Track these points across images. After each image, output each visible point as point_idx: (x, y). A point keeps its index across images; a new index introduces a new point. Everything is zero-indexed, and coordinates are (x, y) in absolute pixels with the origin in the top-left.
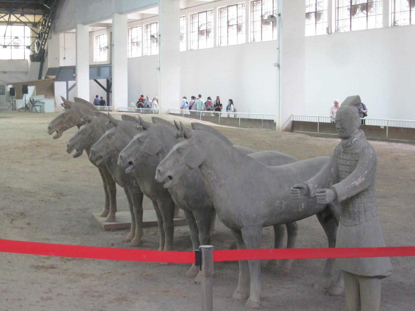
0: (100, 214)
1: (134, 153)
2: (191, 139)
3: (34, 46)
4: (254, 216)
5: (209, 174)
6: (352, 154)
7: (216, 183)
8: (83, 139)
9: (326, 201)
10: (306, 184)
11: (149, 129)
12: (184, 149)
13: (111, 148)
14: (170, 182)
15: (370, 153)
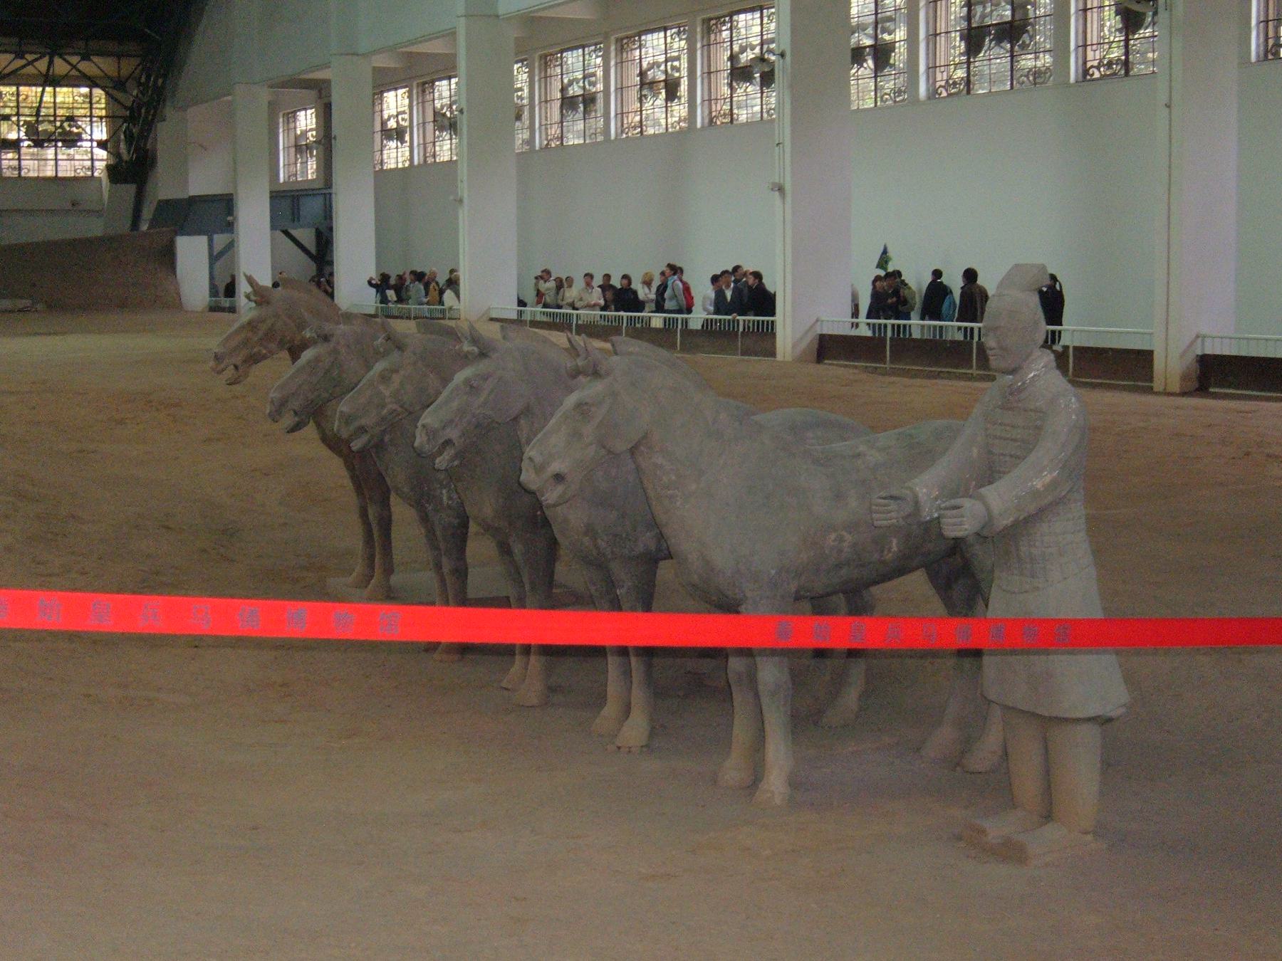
0: (350, 579)
3: (119, 141)
4: (773, 572)
9: (966, 530)
13: (390, 406)
14: (560, 489)
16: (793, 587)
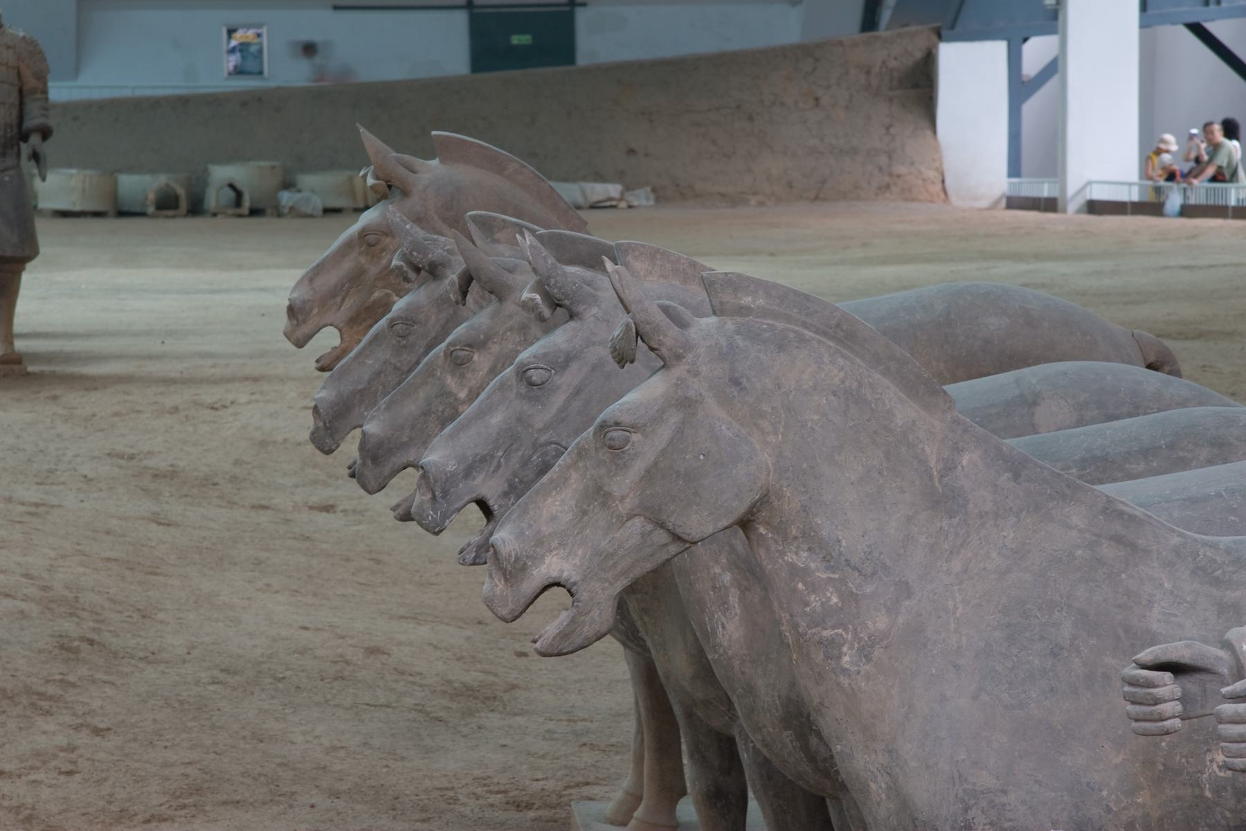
0: (608, 808)
2: (679, 371)
5: (794, 571)
7: (840, 631)
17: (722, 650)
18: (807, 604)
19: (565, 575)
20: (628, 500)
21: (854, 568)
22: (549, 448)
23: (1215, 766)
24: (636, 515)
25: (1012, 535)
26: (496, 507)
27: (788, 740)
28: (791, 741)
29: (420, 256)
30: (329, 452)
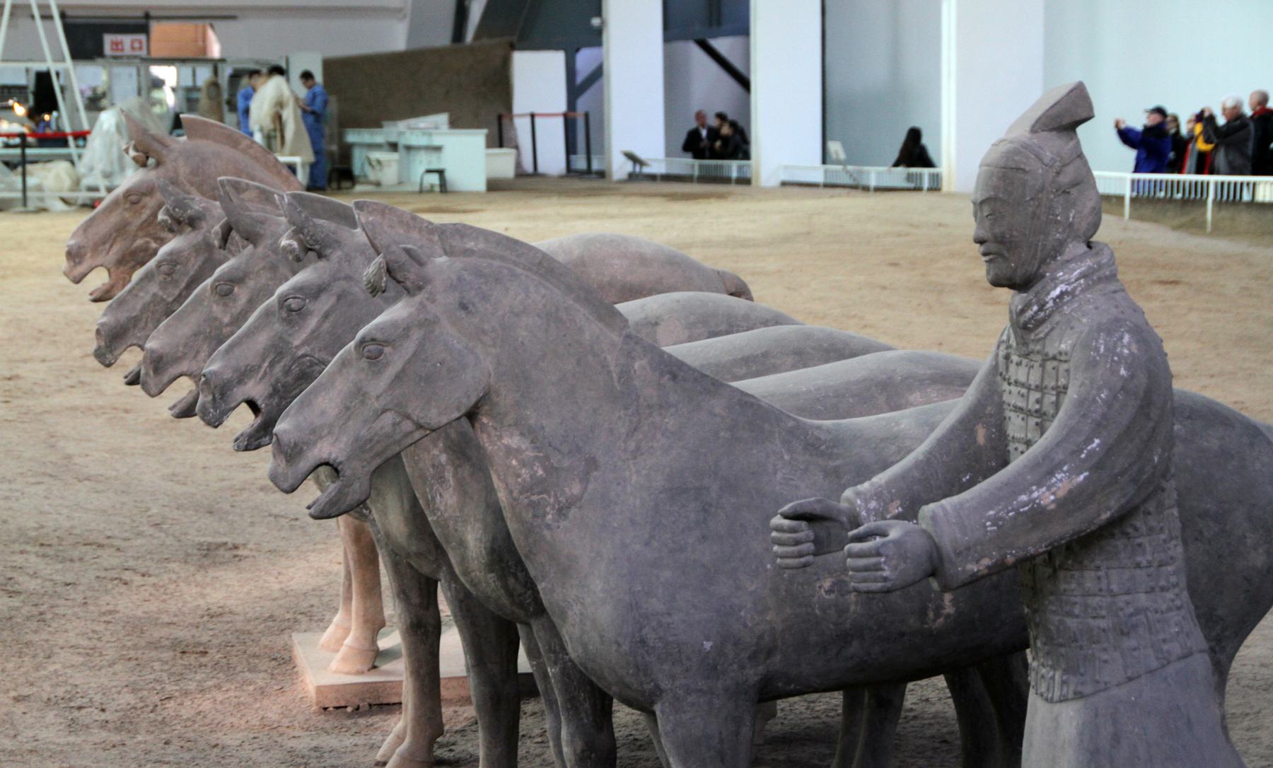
1: (266, 364)
2: (419, 298)
4: (708, 645)
6: (1046, 359)
7: (545, 496)
8: (163, 300)
9: (885, 579)
10: (848, 500)
11: (336, 255)
12: (385, 341)
15: (1120, 355)
16: (753, 674)
17: (439, 514)
18: (519, 476)
19: (333, 456)
20: (381, 398)
21: (555, 448)
22: (304, 360)
23: (822, 591)
24: (388, 410)
25: (672, 421)
26: (263, 406)
27: (491, 581)
28: (494, 581)
29: (182, 212)
30: (109, 365)
